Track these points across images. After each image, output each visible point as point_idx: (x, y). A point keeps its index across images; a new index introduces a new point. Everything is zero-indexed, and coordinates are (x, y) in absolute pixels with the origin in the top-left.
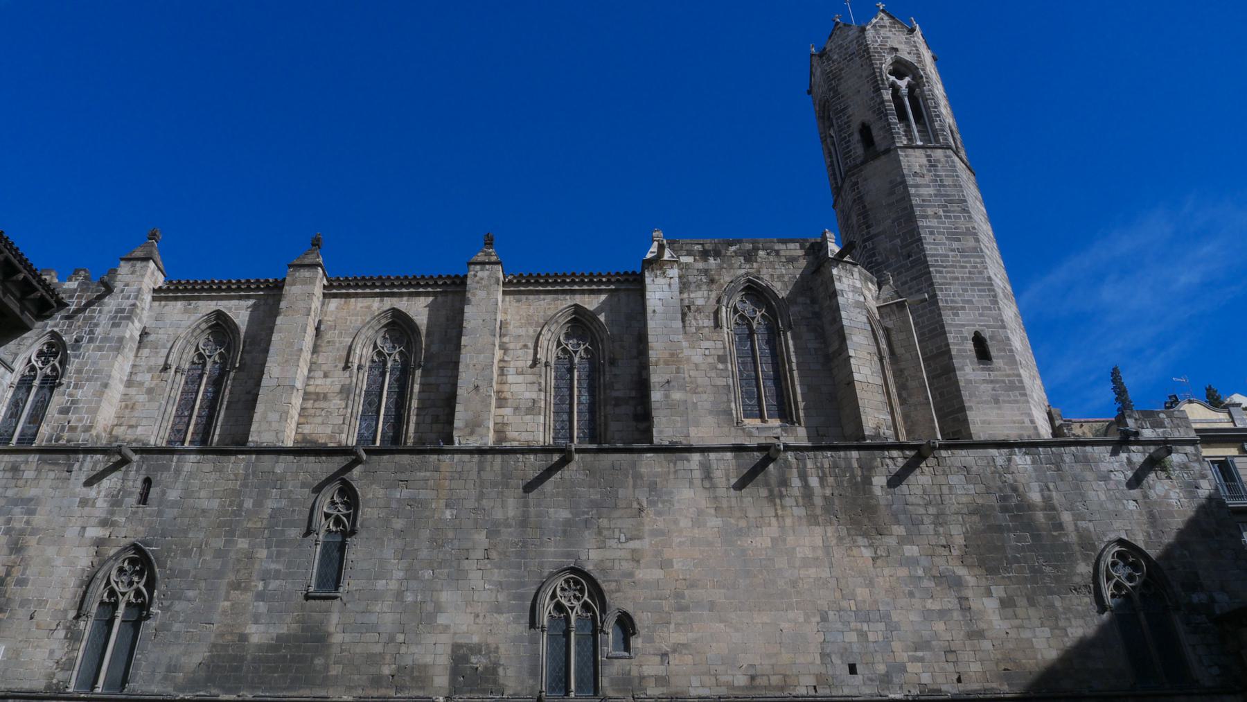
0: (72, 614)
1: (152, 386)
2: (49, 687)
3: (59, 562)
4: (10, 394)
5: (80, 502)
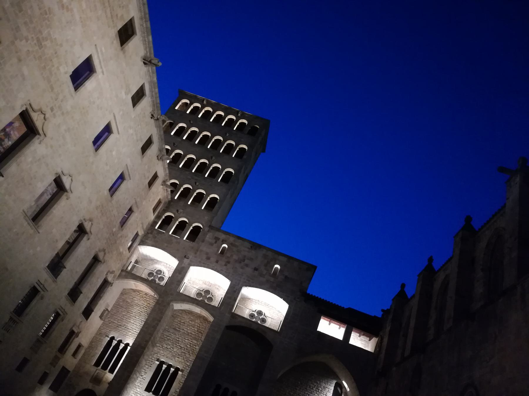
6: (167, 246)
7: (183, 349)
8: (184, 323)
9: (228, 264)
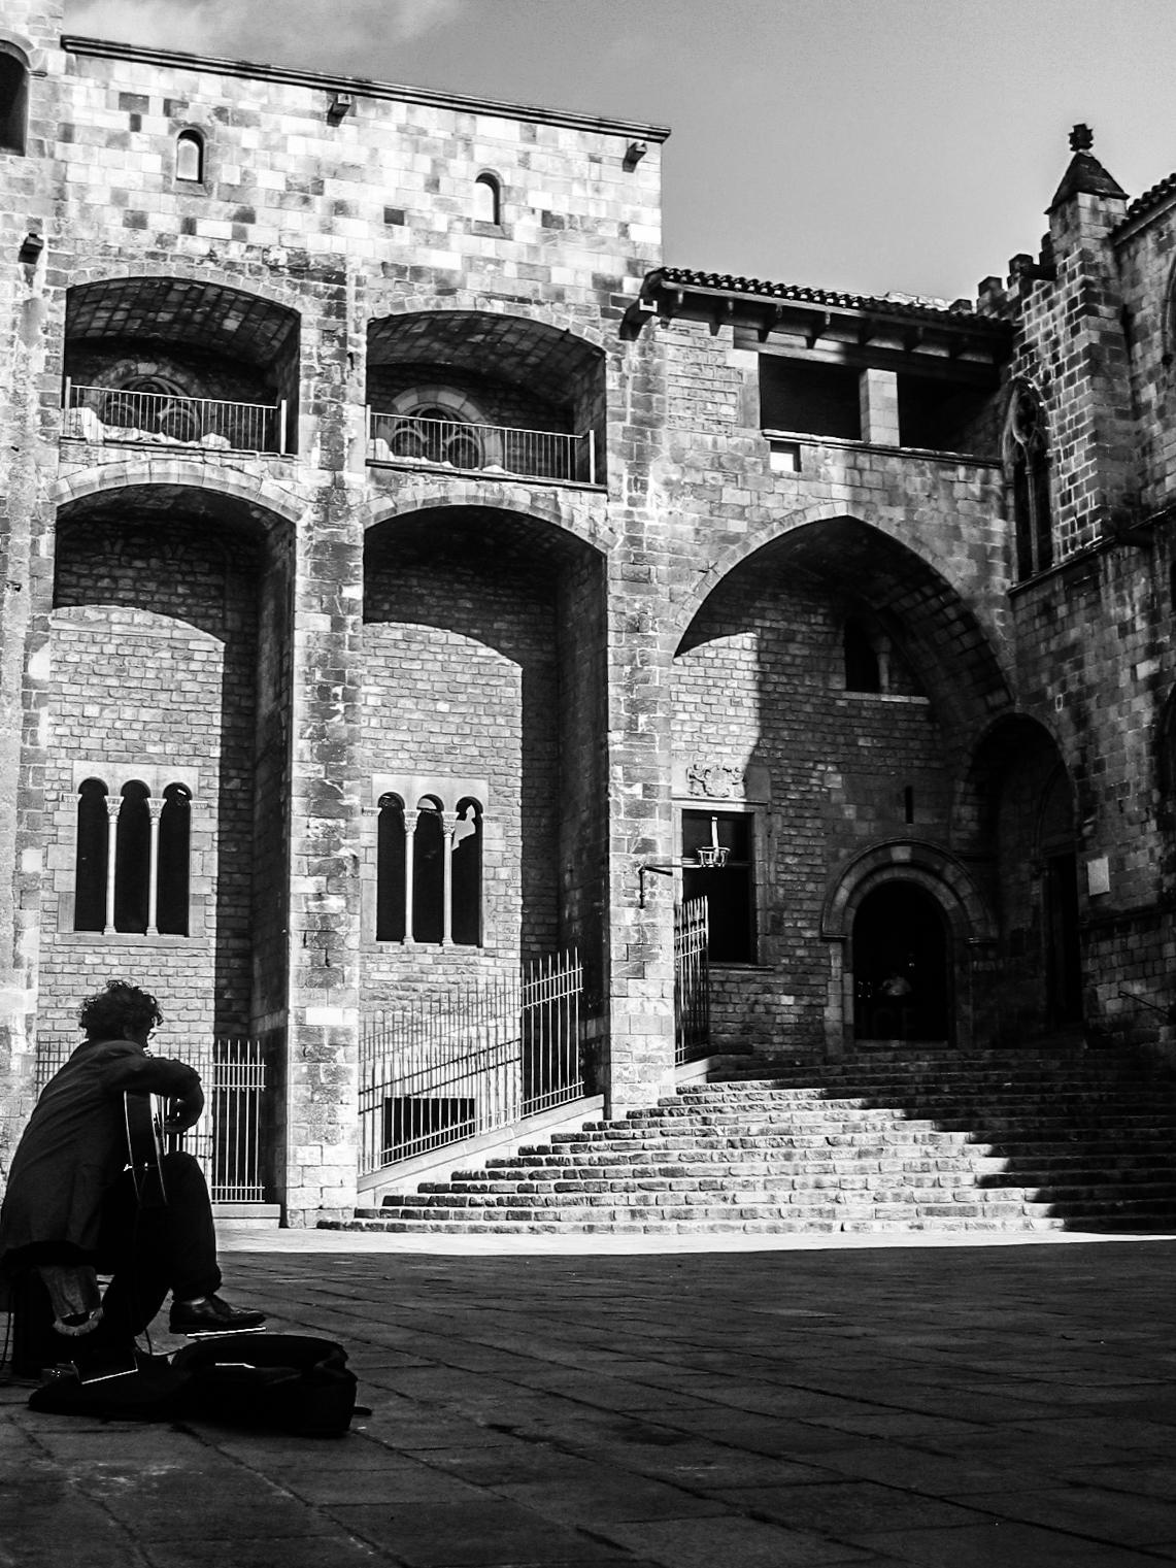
0: (1156, 796)
1: (1161, 403)
2: (1161, 897)
3: (1123, 727)
4: (1011, 501)
5: (1120, 630)
7: (163, 696)
8: (115, 579)
9: (249, 226)
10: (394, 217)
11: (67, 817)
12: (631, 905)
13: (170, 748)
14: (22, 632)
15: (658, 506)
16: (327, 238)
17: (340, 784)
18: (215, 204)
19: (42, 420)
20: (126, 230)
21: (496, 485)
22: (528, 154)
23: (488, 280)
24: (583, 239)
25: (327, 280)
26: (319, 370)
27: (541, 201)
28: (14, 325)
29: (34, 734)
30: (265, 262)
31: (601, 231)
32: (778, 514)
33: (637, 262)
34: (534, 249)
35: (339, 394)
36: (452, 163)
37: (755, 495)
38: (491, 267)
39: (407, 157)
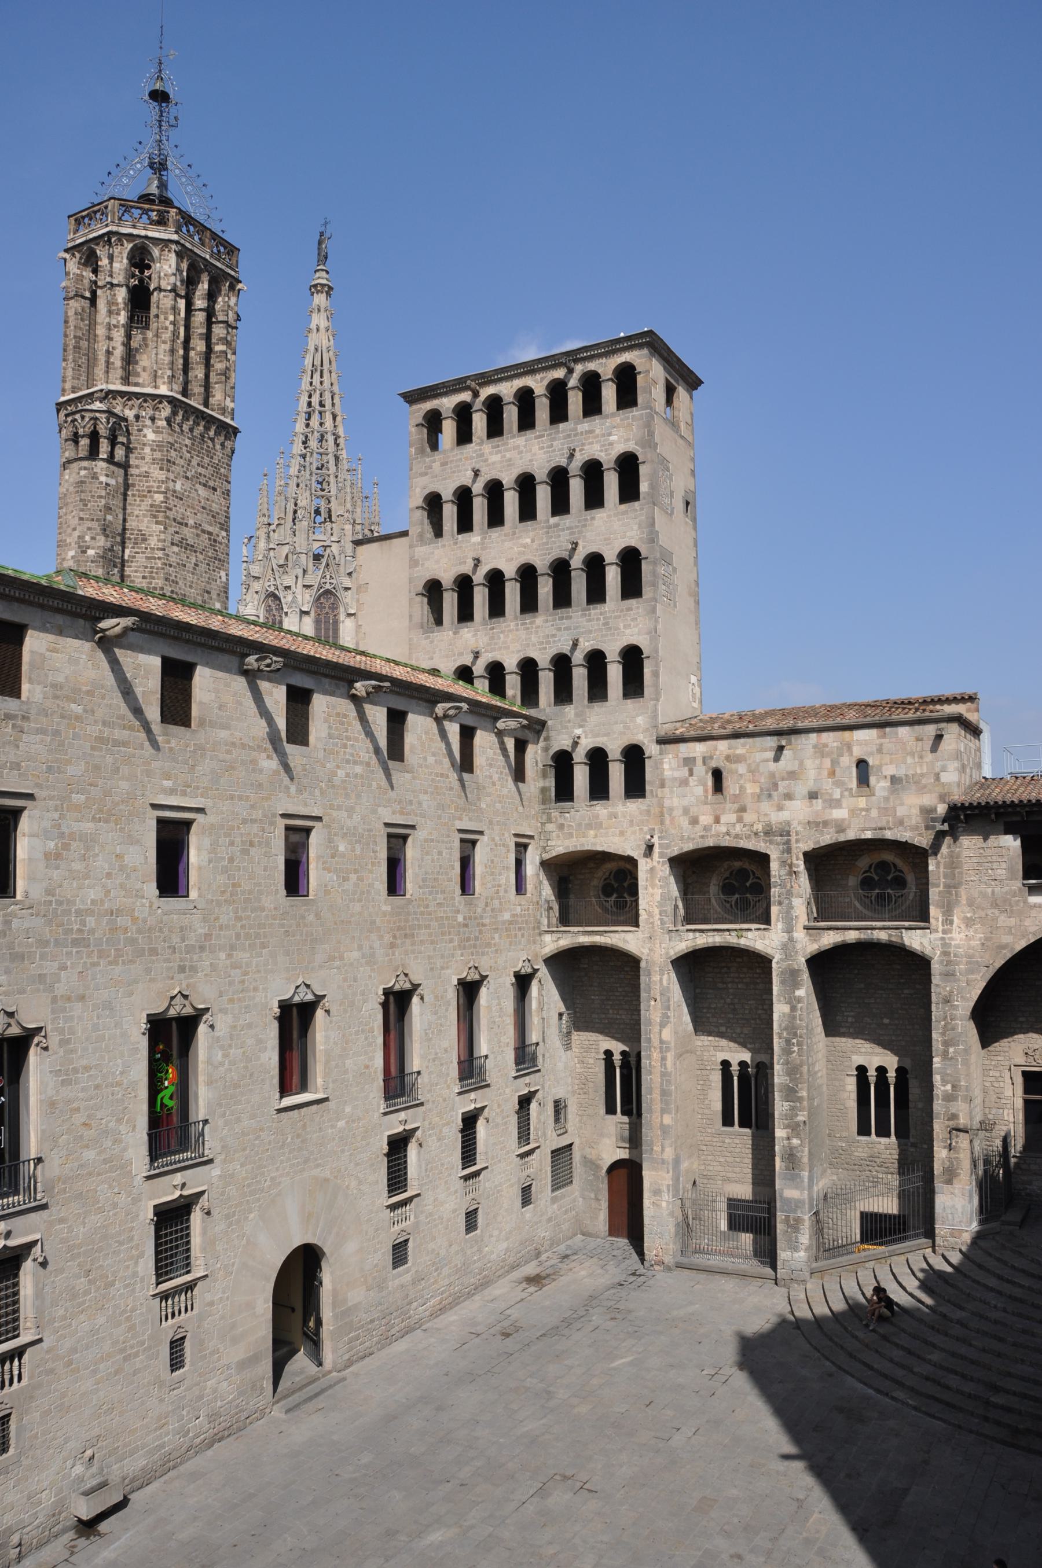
6: (596, 836)
7: (752, 1022)
8: (729, 968)
9: (745, 815)
10: (813, 796)
11: (717, 1078)
12: (945, 1147)
13: (757, 1045)
14: (658, 1020)
15: (959, 933)
16: (780, 813)
17: (797, 1086)
18: (728, 806)
19: (661, 924)
20: (690, 826)
21: (869, 931)
22: (881, 745)
23: (862, 821)
24: (914, 787)
25: (781, 836)
26: (779, 883)
27: (890, 770)
28: (647, 880)
29: (665, 1065)
30: (752, 832)
31: (924, 781)
32: (1032, 929)
33: (945, 794)
34: (886, 799)
35: (789, 894)
36: (842, 759)
37: (1018, 919)
38: (864, 813)
39: (818, 761)
